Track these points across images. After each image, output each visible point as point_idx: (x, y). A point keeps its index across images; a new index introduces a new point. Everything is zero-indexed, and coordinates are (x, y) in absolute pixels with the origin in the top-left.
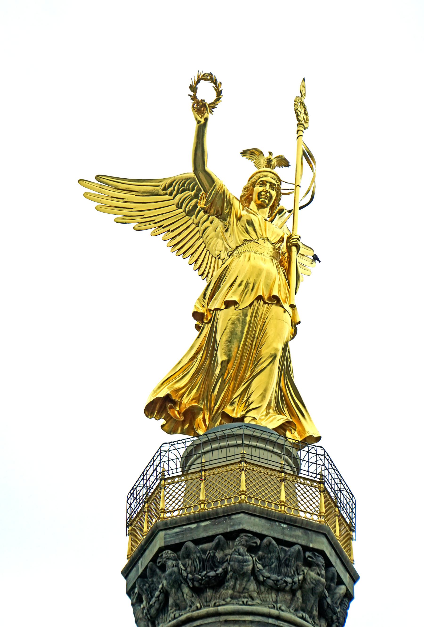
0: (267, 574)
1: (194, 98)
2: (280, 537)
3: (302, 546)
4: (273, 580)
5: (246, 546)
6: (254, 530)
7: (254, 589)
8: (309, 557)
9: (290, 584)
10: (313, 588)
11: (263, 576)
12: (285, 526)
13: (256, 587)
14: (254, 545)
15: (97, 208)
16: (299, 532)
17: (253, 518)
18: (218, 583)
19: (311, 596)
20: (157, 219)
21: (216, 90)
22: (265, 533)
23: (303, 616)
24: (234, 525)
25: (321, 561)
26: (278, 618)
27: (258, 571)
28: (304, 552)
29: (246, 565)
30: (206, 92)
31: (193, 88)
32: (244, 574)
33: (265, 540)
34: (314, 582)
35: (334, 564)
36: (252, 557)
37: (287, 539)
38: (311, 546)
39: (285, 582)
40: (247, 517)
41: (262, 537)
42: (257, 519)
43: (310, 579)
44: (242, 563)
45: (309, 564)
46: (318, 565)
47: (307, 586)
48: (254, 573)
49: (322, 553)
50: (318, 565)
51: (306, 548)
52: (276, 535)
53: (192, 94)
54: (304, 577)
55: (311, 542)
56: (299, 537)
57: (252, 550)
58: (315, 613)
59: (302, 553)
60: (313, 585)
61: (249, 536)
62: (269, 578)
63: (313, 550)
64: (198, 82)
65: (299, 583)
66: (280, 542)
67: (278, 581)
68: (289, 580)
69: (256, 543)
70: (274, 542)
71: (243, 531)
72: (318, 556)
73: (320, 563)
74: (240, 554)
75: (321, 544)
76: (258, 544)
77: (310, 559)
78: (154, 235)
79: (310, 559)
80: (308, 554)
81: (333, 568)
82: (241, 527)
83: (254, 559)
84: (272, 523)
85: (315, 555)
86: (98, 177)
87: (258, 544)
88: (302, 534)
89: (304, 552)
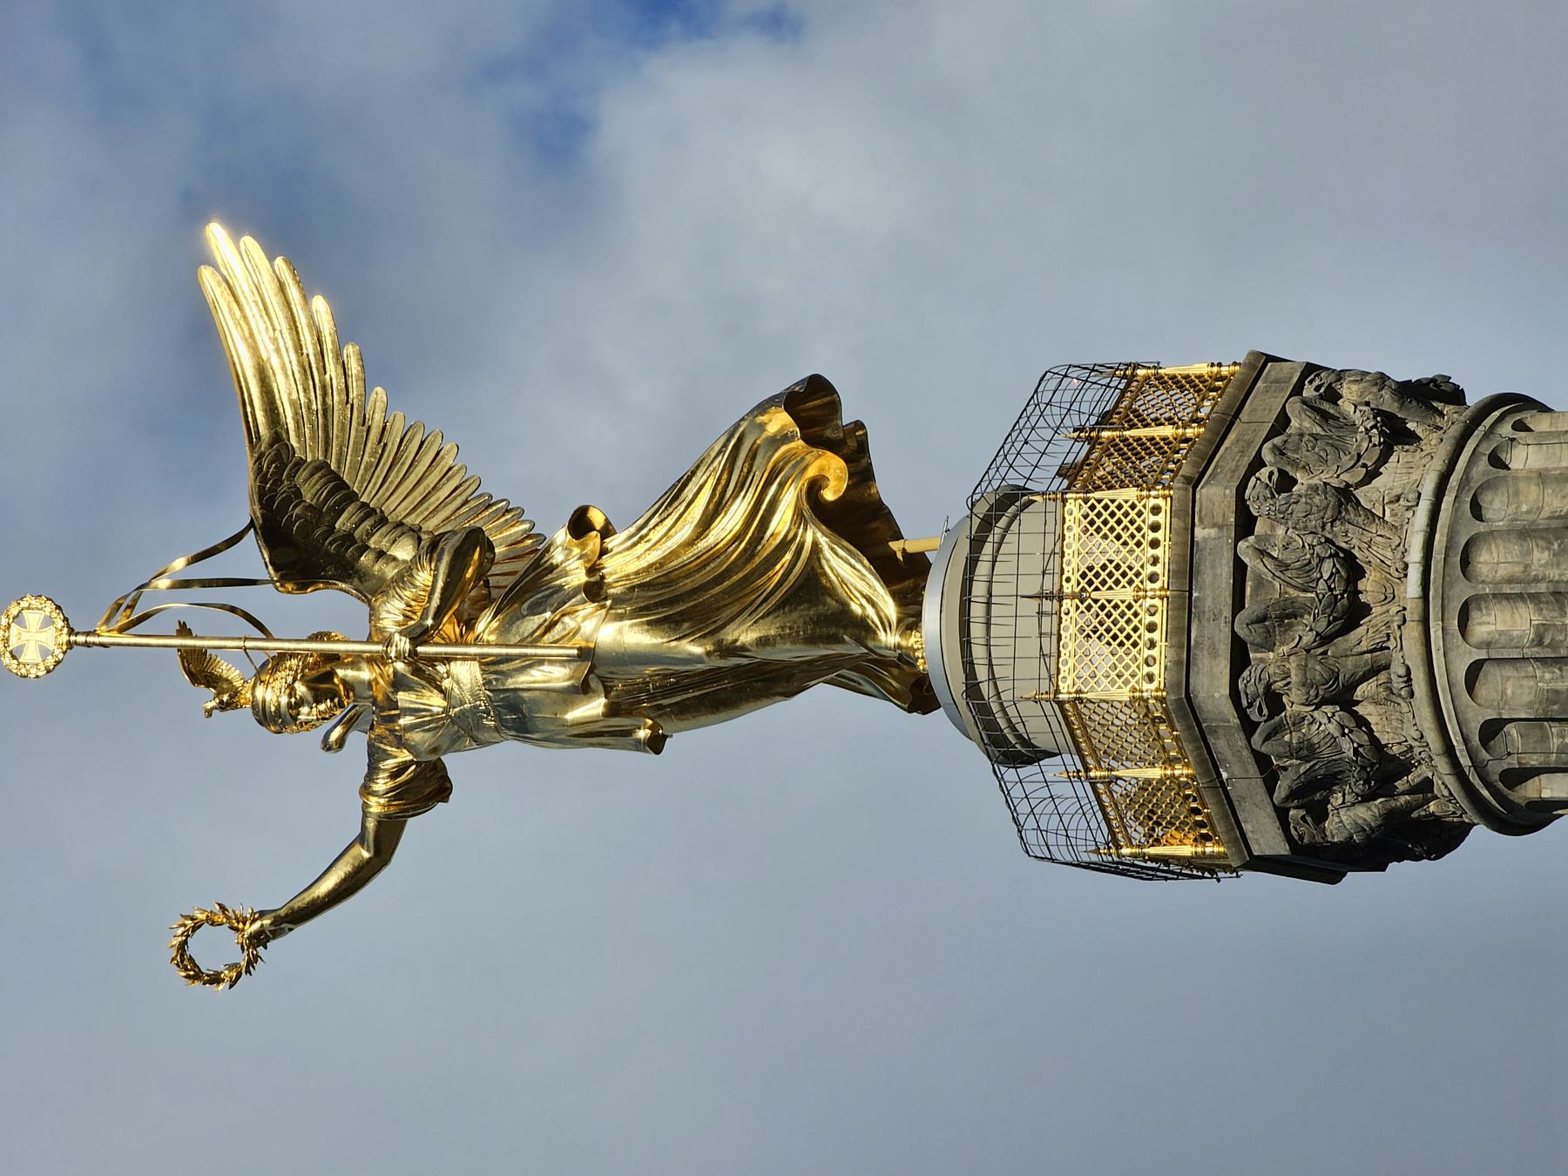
2: (1260, 782)
12: (1225, 775)
14: (1309, 819)
16: (1220, 745)
17: (1249, 835)
22: (1270, 809)
26: (1449, 750)
34: (1313, 692)
35: (1227, 631)
37: (1253, 769)
39: (1356, 752)
41: (1281, 814)
45: (1274, 702)
49: (1234, 694)
51: (1249, 727)
57: (1319, 813)
58: (1363, 636)
66: (1270, 777)
69: (1303, 818)
76: (1303, 812)
77: (1265, 711)
79: (1265, 711)
80: (1255, 717)
81: (1241, 631)
85: (1250, 705)
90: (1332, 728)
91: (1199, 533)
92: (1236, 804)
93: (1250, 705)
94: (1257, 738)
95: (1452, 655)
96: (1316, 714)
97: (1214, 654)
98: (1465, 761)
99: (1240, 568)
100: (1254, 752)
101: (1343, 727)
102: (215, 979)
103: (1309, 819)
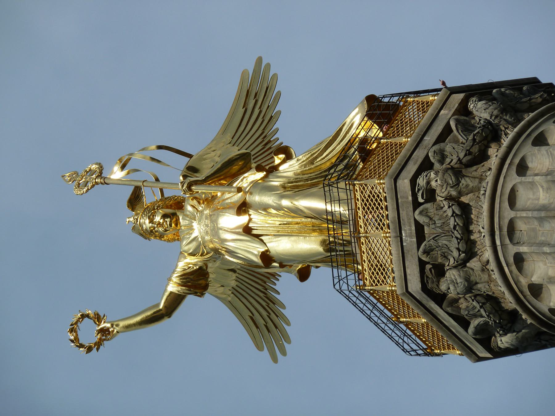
0: (456, 253)
1: (98, 344)
3: (414, 210)
4: (459, 243)
5: (438, 282)
6: (419, 275)
7: (477, 261)
8: (422, 198)
9: (455, 221)
10: (452, 187)
11: (460, 255)
13: (475, 259)
14: (433, 271)
15: (289, 342)
16: (403, 214)
17: (408, 277)
18: (492, 301)
19: (461, 184)
20: (262, 295)
21: (82, 320)
23: (483, 194)
24: (424, 298)
25: (421, 181)
27: (457, 262)
28: (422, 204)
29: (456, 280)
30: (89, 333)
31: (89, 349)
32: (467, 279)
33: (424, 258)
36: (447, 270)
38: (410, 198)
40: (409, 285)
41: (422, 264)
42: (408, 271)
43: (443, 193)
44: (456, 285)
46: (428, 183)
47: (454, 193)
48: (462, 264)
49: (413, 181)
50: (428, 183)
51: (416, 205)
52: (415, 246)
53: (95, 349)
54: (445, 200)
55: (408, 198)
56: (408, 215)
57: (440, 271)
59: (421, 208)
60: (448, 189)
61: (427, 281)
62: (458, 249)
63: (414, 195)
64: (81, 346)
65: (453, 205)
67: (457, 238)
68: (452, 222)
69: (430, 269)
70: (421, 250)
71: (425, 288)
72: (419, 185)
73: (425, 181)
74: (449, 288)
75: (404, 184)
76: (431, 266)
78: (278, 293)
80: (421, 200)
82: (421, 292)
83: (448, 268)
84: (405, 251)
86: (260, 348)
87: (431, 266)
88: (403, 210)
89: (422, 204)
90: (450, 213)
91: (442, 112)
92: (405, 255)
93: (419, 190)
94: (417, 212)
95: (508, 179)
96: (445, 202)
97: (415, 164)
98: (498, 242)
99: (447, 130)
100: (416, 222)
101: (454, 212)
102: (81, 346)
103: (433, 271)
